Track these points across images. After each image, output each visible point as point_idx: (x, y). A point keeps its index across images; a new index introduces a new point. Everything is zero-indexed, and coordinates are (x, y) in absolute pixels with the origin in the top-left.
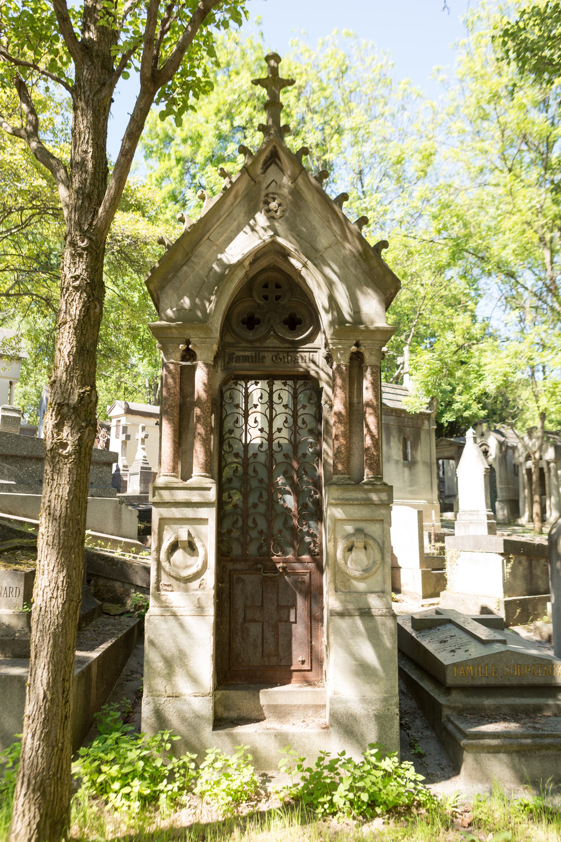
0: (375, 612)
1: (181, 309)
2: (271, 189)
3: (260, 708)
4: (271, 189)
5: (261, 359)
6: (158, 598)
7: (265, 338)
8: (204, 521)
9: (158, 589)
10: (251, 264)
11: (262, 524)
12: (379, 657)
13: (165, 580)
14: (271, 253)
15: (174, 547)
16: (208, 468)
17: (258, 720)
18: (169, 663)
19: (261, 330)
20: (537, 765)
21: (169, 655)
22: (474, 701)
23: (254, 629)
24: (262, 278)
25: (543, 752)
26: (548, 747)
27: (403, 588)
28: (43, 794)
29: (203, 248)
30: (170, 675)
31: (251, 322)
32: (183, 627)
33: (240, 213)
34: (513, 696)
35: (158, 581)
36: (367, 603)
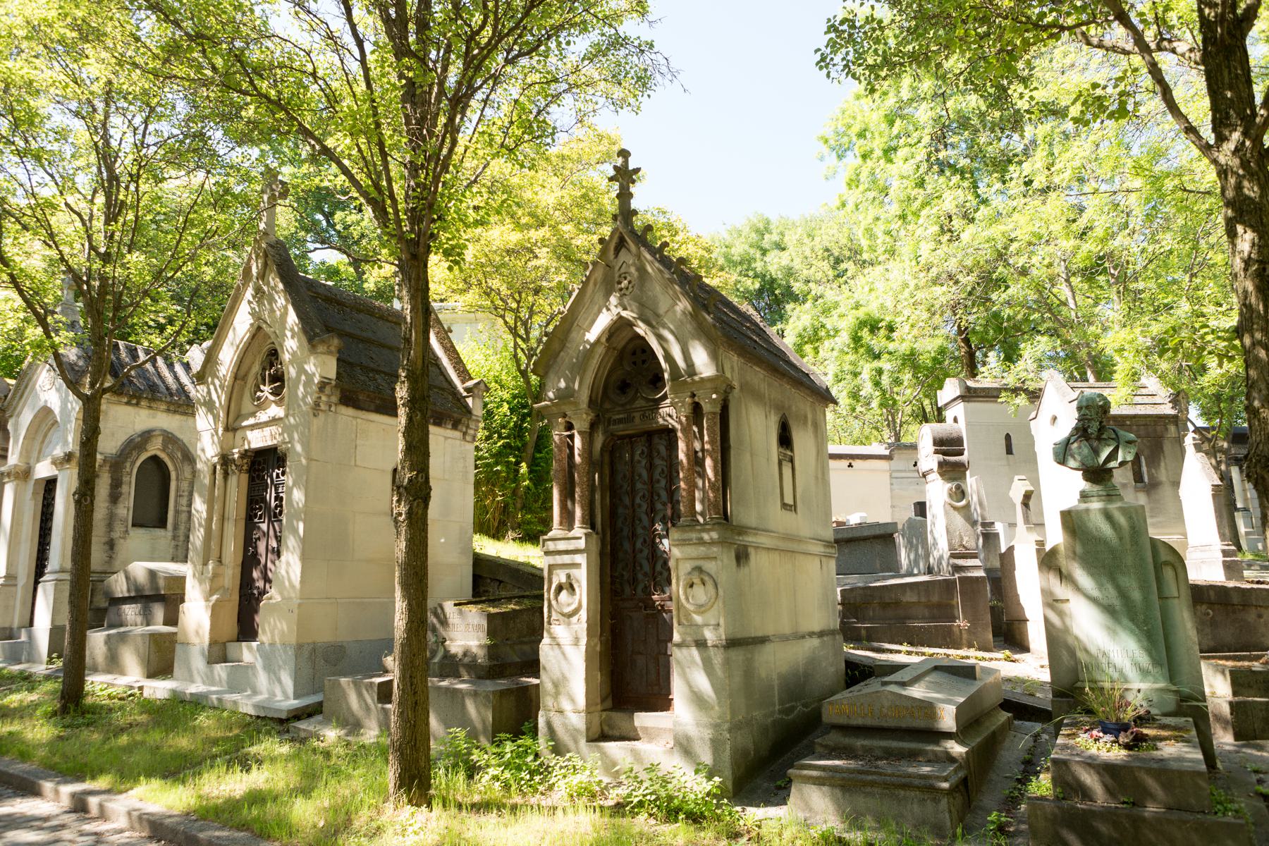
0: (710, 643)
1: (559, 390)
2: (623, 270)
3: (635, 729)
4: (623, 270)
5: (630, 419)
6: (549, 632)
7: (634, 399)
8: (577, 566)
9: (550, 623)
10: (608, 340)
11: (647, 567)
12: (713, 685)
13: (554, 616)
14: (620, 325)
15: (560, 588)
16: (583, 522)
17: (629, 739)
18: (556, 685)
19: (631, 393)
20: (861, 801)
21: (555, 678)
22: (847, 741)
23: (641, 661)
24: (631, 346)
25: (868, 789)
26: (872, 784)
27: (1032, 646)
28: (402, 754)
29: (574, 335)
30: (557, 694)
31: (624, 387)
32: (567, 655)
33: (599, 297)
34: (893, 739)
35: (550, 617)
36: (703, 635)
